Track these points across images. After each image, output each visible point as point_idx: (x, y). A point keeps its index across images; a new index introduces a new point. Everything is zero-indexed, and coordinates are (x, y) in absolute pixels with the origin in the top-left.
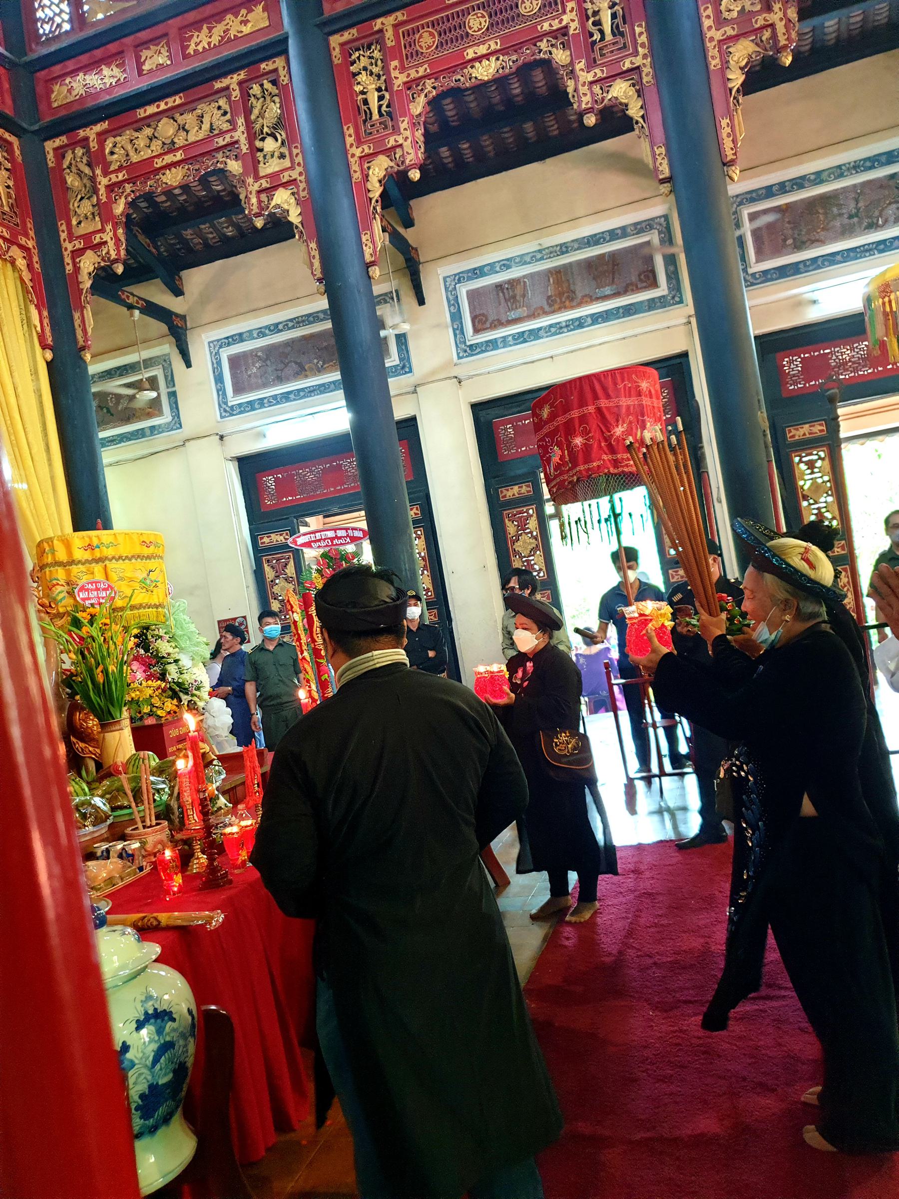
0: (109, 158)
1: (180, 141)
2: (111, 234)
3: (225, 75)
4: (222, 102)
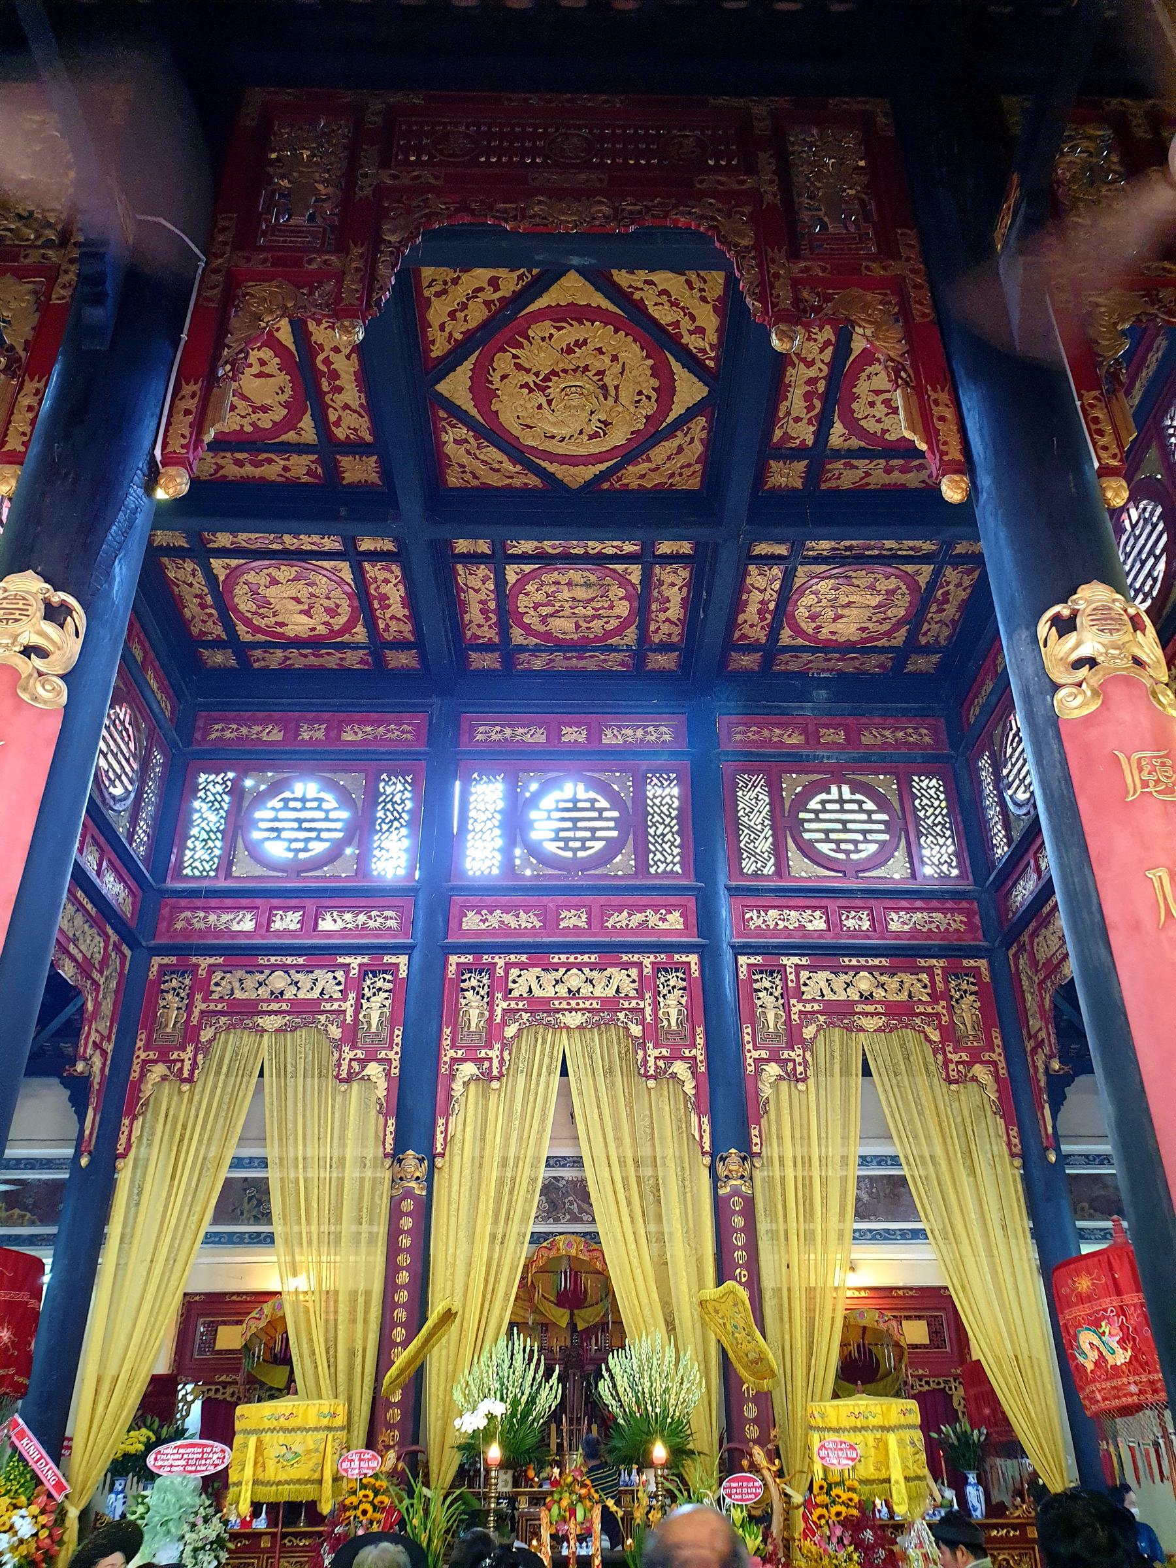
2: (191, 1055)
3: (350, 955)
4: (340, 974)
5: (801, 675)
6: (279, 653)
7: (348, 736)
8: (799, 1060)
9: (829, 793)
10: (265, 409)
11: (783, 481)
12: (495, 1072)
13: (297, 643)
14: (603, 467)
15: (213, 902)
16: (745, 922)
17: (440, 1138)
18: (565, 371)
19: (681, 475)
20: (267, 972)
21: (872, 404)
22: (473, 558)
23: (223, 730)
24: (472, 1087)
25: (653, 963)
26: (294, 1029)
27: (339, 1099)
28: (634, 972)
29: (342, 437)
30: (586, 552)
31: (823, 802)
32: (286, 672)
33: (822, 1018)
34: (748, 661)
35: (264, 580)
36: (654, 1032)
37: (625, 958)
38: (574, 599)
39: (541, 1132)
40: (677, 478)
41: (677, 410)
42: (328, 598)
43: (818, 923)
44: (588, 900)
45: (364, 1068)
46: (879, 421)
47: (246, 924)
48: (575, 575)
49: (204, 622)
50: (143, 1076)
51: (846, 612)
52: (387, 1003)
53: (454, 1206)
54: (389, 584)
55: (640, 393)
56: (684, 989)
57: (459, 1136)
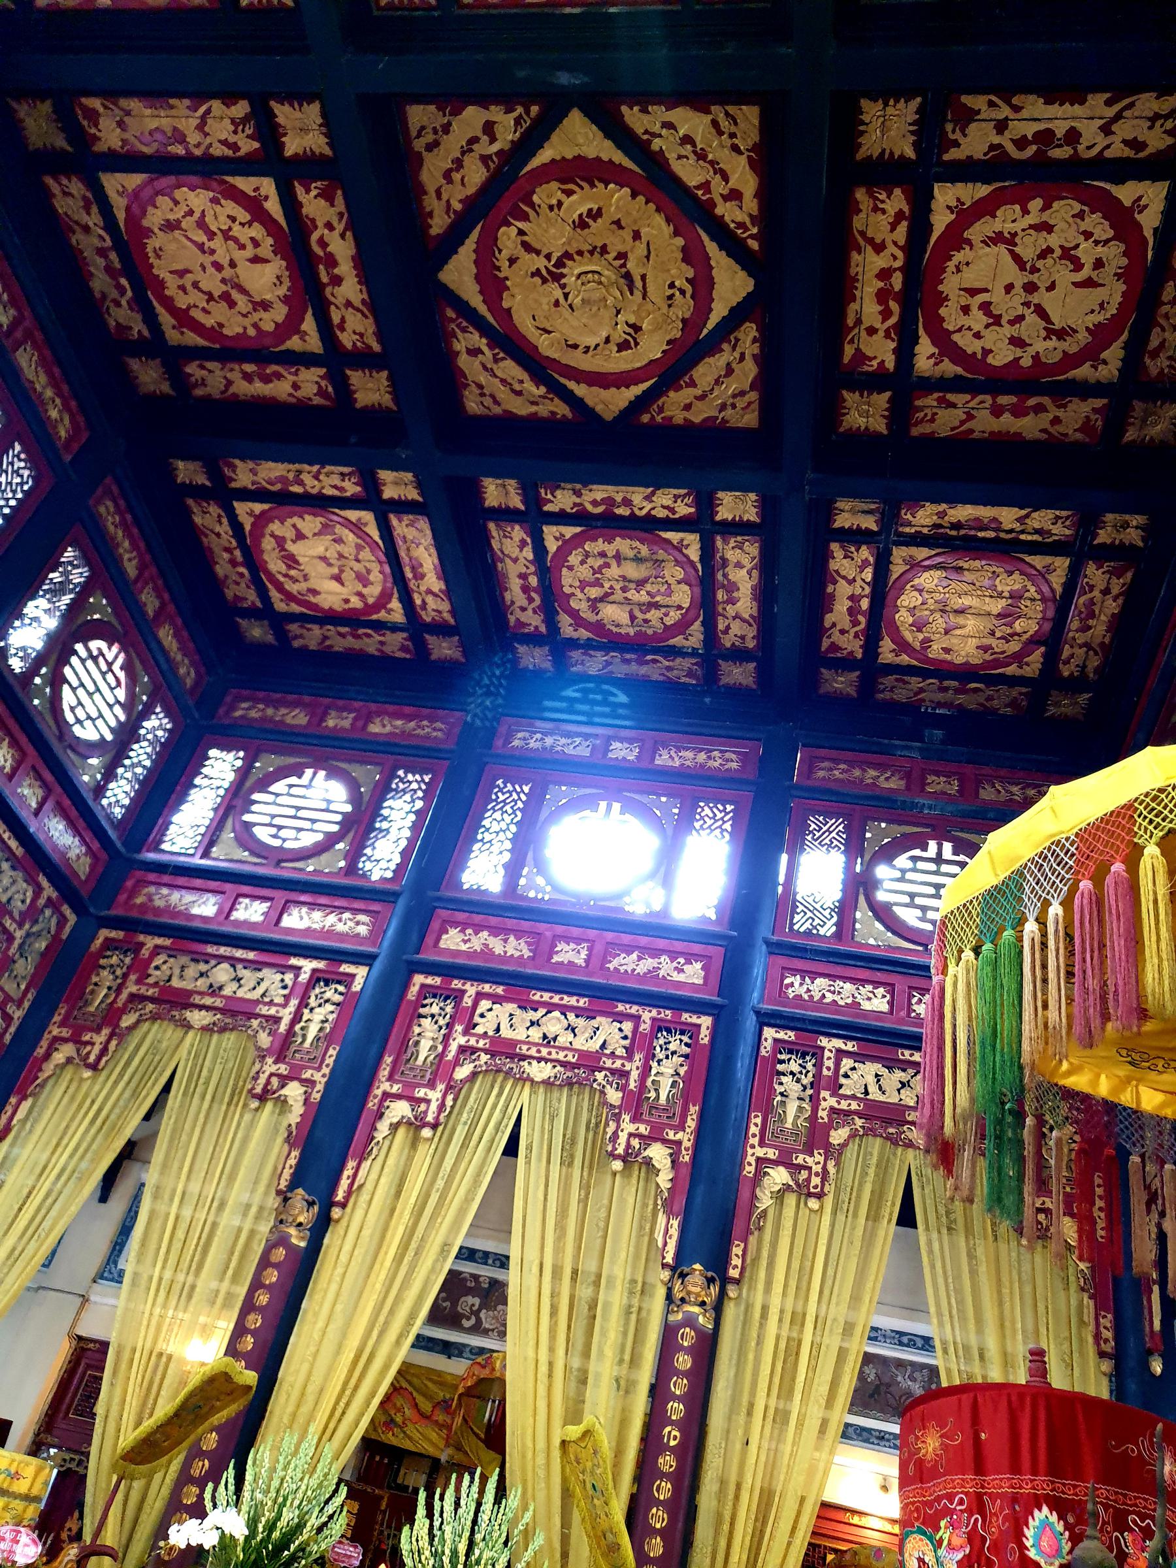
0: (151, 971)
1: (227, 991)
3: (306, 957)
5: (911, 708)
6: (316, 631)
7: (375, 728)
8: (817, 1168)
9: (925, 849)
10: (265, 306)
11: (862, 422)
12: (430, 1118)
13: (330, 618)
14: (637, 390)
15: (181, 881)
16: (782, 988)
17: (344, 1183)
18: (580, 253)
19: (734, 406)
20: (213, 962)
21: (966, 310)
22: (505, 515)
23: (248, 709)
24: (401, 1131)
25: (654, 1020)
26: (223, 1030)
27: (247, 1117)
28: (628, 1026)
29: (349, 346)
30: (633, 513)
31: (914, 859)
32: (325, 657)
33: (859, 1122)
34: (842, 683)
35: (289, 534)
36: (636, 1104)
37: (621, 1007)
38: (624, 578)
39: (468, 1200)
40: (729, 412)
41: (719, 311)
42: (358, 560)
43: (876, 1002)
44: (592, 934)
45: (283, 1087)
46: (977, 335)
47: (205, 907)
48: (622, 545)
49: (238, 584)
50: (47, 1056)
51: (960, 620)
52: (331, 1017)
53: (340, 1270)
54: (419, 543)
55: (672, 286)
56: (686, 1056)
57: (369, 1186)
